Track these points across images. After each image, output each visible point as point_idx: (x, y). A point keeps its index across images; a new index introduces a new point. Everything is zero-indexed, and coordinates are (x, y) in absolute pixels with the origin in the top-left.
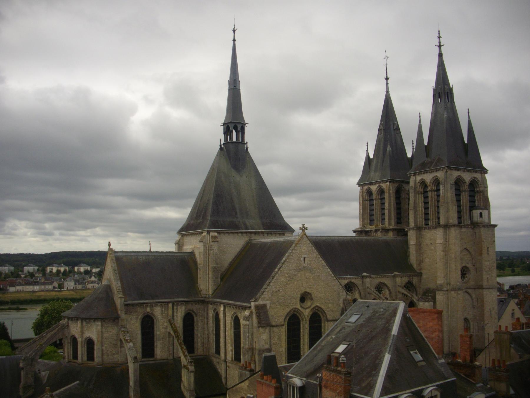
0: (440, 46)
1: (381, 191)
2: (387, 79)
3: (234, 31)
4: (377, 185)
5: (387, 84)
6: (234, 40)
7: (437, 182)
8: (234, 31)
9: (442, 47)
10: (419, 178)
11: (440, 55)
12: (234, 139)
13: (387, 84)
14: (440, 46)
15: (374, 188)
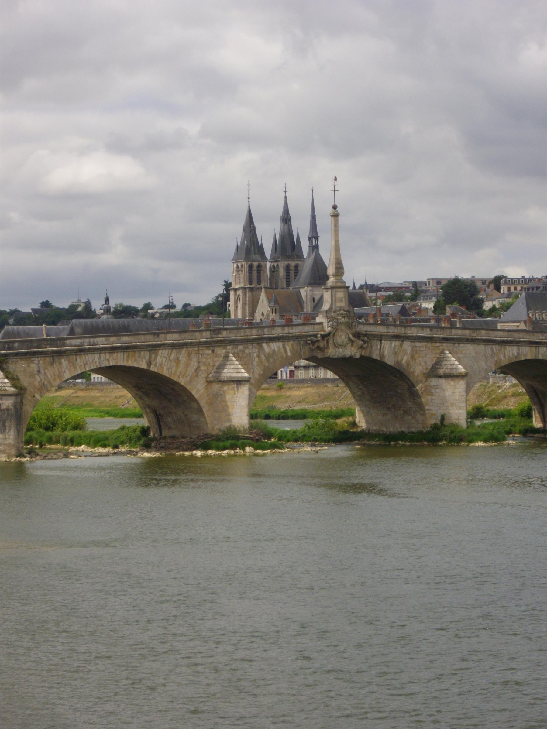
0: (285, 192)
1: (259, 266)
2: (249, 198)
3: (312, 190)
4: (258, 263)
5: (249, 202)
6: (313, 195)
7: (296, 266)
8: (312, 190)
9: (287, 193)
10: (286, 263)
11: (286, 197)
12: (314, 244)
13: (249, 202)
14: (285, 192)
15: (255, 264)
